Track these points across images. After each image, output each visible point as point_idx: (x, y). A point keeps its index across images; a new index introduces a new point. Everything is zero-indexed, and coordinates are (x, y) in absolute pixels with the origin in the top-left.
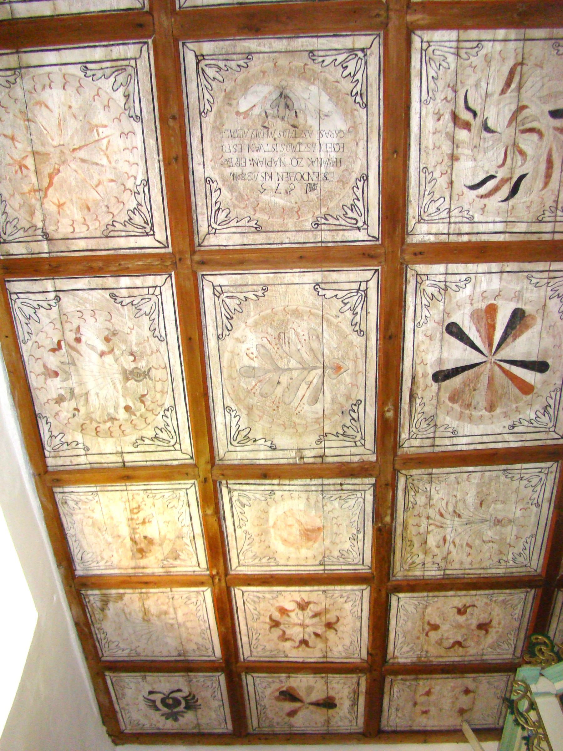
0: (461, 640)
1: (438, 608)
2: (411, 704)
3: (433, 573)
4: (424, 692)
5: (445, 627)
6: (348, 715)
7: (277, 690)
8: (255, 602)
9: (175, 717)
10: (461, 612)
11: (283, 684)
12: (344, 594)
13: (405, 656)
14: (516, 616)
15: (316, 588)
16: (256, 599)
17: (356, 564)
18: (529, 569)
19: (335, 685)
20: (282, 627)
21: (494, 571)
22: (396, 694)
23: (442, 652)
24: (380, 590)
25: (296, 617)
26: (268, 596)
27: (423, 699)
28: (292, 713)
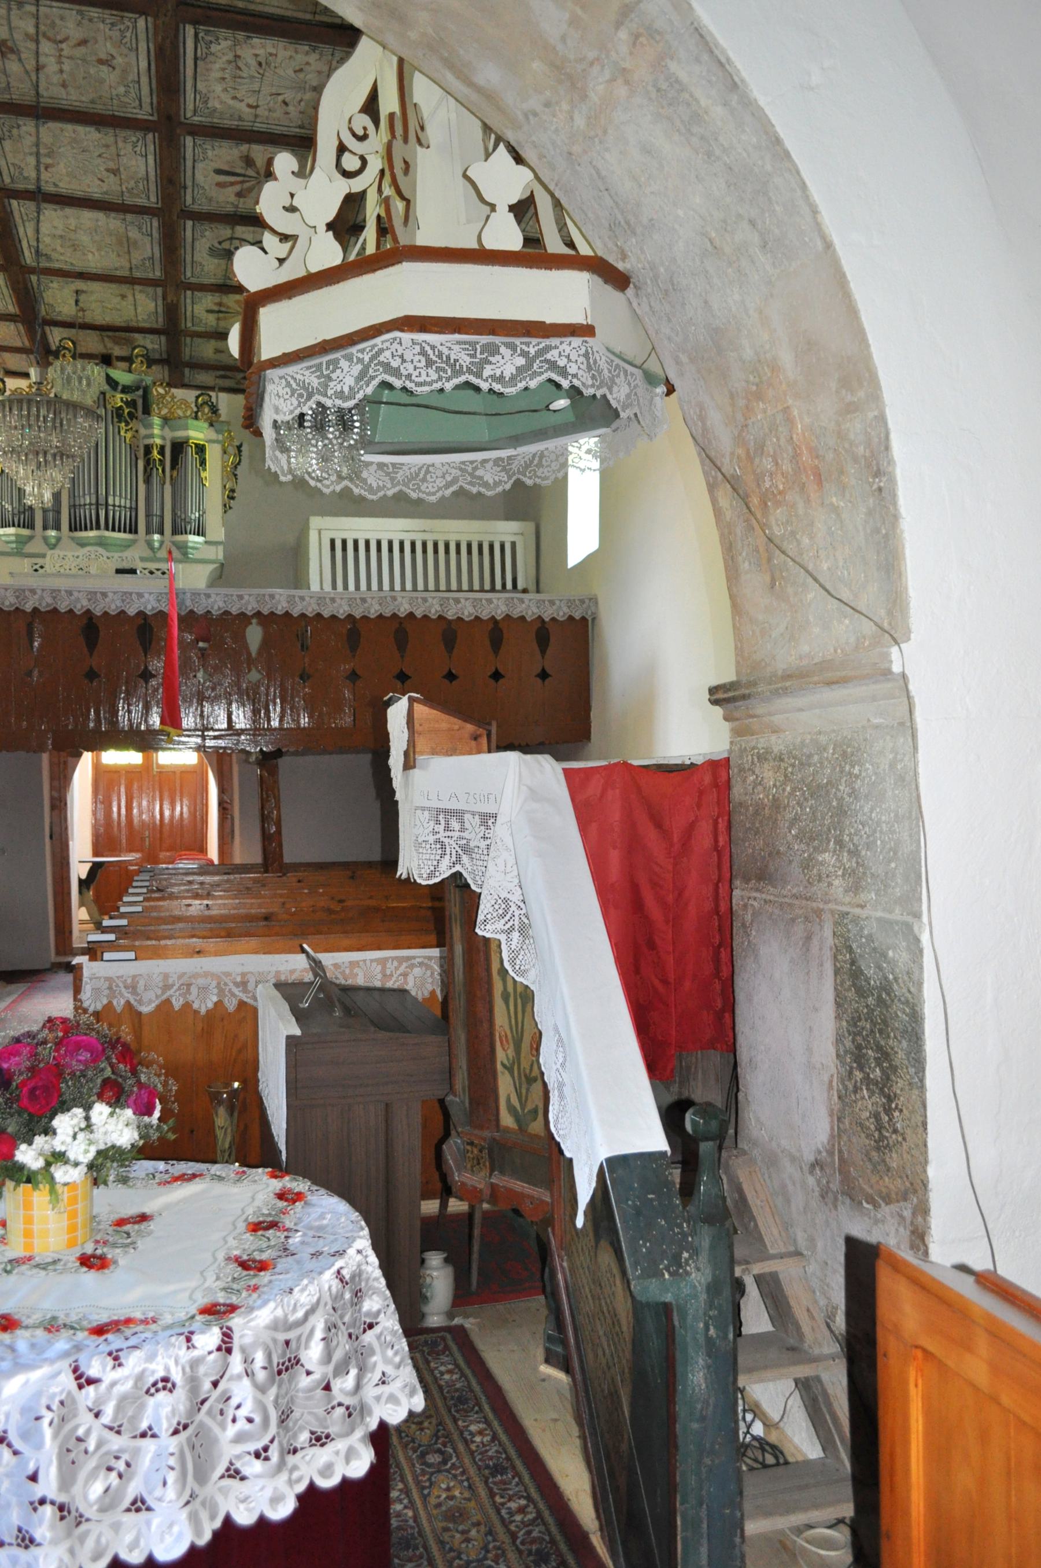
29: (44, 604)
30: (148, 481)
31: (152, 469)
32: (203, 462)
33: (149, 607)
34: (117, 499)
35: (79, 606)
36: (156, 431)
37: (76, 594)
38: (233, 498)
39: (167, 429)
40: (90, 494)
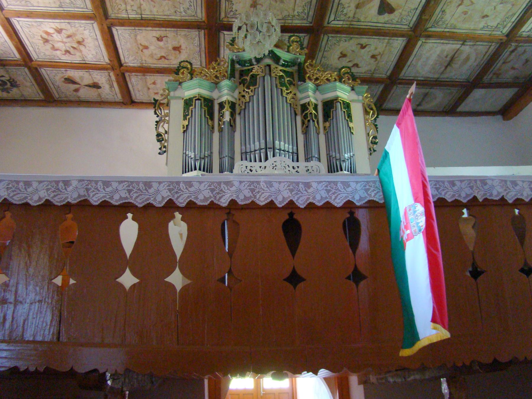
0: (165, 56)
1: (144, 37)
2: (146, 89)
3: (134, 16)
4: (151, 83)
5: (152, 48)
6: (111, 93)
7: (62, 77)
8: (28, 27)
9: (7, 91)
10: (160, 39)
11: (64, 75)
12: (82, 25)
13: (133, 62)
14: (196, 44)
15: (62, 21)
16: (28, 26)
17: (82, 8)
18: (196, 18)
19: (96, 76)
20: (51, 42)
21: (173, 17)
22: (134, 83)
23: (155, 62)
24: (102, 25)
25: (56, 37)
26: (35, 24)
27: (153, 86)
28: (77, 90)
29: (242, 197)
30: (306, 132)
31: (309, 121)
32: (350, 116)
33: (357, 197)
34: (282, 143)
35: (280, 198)
36: (310, 93)
37: (276, 185)
38: (376, 143)
39: (317, 93)
40: (259, 141)
